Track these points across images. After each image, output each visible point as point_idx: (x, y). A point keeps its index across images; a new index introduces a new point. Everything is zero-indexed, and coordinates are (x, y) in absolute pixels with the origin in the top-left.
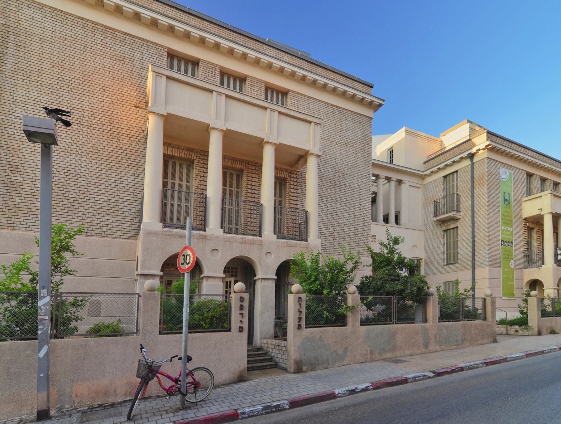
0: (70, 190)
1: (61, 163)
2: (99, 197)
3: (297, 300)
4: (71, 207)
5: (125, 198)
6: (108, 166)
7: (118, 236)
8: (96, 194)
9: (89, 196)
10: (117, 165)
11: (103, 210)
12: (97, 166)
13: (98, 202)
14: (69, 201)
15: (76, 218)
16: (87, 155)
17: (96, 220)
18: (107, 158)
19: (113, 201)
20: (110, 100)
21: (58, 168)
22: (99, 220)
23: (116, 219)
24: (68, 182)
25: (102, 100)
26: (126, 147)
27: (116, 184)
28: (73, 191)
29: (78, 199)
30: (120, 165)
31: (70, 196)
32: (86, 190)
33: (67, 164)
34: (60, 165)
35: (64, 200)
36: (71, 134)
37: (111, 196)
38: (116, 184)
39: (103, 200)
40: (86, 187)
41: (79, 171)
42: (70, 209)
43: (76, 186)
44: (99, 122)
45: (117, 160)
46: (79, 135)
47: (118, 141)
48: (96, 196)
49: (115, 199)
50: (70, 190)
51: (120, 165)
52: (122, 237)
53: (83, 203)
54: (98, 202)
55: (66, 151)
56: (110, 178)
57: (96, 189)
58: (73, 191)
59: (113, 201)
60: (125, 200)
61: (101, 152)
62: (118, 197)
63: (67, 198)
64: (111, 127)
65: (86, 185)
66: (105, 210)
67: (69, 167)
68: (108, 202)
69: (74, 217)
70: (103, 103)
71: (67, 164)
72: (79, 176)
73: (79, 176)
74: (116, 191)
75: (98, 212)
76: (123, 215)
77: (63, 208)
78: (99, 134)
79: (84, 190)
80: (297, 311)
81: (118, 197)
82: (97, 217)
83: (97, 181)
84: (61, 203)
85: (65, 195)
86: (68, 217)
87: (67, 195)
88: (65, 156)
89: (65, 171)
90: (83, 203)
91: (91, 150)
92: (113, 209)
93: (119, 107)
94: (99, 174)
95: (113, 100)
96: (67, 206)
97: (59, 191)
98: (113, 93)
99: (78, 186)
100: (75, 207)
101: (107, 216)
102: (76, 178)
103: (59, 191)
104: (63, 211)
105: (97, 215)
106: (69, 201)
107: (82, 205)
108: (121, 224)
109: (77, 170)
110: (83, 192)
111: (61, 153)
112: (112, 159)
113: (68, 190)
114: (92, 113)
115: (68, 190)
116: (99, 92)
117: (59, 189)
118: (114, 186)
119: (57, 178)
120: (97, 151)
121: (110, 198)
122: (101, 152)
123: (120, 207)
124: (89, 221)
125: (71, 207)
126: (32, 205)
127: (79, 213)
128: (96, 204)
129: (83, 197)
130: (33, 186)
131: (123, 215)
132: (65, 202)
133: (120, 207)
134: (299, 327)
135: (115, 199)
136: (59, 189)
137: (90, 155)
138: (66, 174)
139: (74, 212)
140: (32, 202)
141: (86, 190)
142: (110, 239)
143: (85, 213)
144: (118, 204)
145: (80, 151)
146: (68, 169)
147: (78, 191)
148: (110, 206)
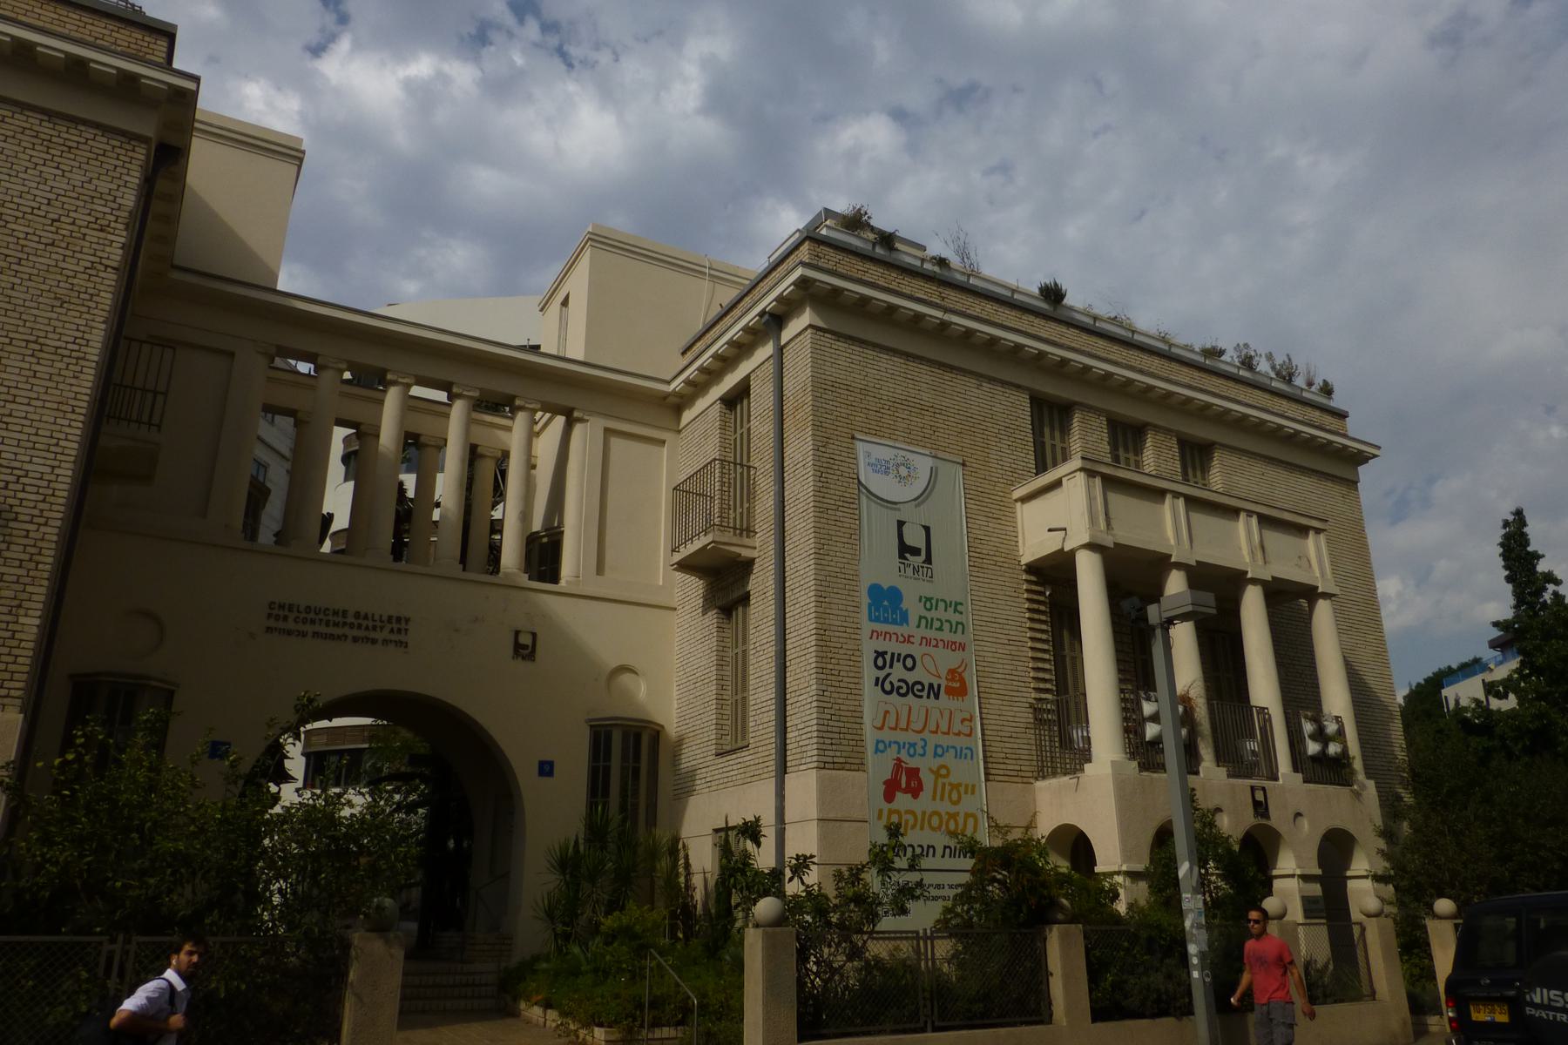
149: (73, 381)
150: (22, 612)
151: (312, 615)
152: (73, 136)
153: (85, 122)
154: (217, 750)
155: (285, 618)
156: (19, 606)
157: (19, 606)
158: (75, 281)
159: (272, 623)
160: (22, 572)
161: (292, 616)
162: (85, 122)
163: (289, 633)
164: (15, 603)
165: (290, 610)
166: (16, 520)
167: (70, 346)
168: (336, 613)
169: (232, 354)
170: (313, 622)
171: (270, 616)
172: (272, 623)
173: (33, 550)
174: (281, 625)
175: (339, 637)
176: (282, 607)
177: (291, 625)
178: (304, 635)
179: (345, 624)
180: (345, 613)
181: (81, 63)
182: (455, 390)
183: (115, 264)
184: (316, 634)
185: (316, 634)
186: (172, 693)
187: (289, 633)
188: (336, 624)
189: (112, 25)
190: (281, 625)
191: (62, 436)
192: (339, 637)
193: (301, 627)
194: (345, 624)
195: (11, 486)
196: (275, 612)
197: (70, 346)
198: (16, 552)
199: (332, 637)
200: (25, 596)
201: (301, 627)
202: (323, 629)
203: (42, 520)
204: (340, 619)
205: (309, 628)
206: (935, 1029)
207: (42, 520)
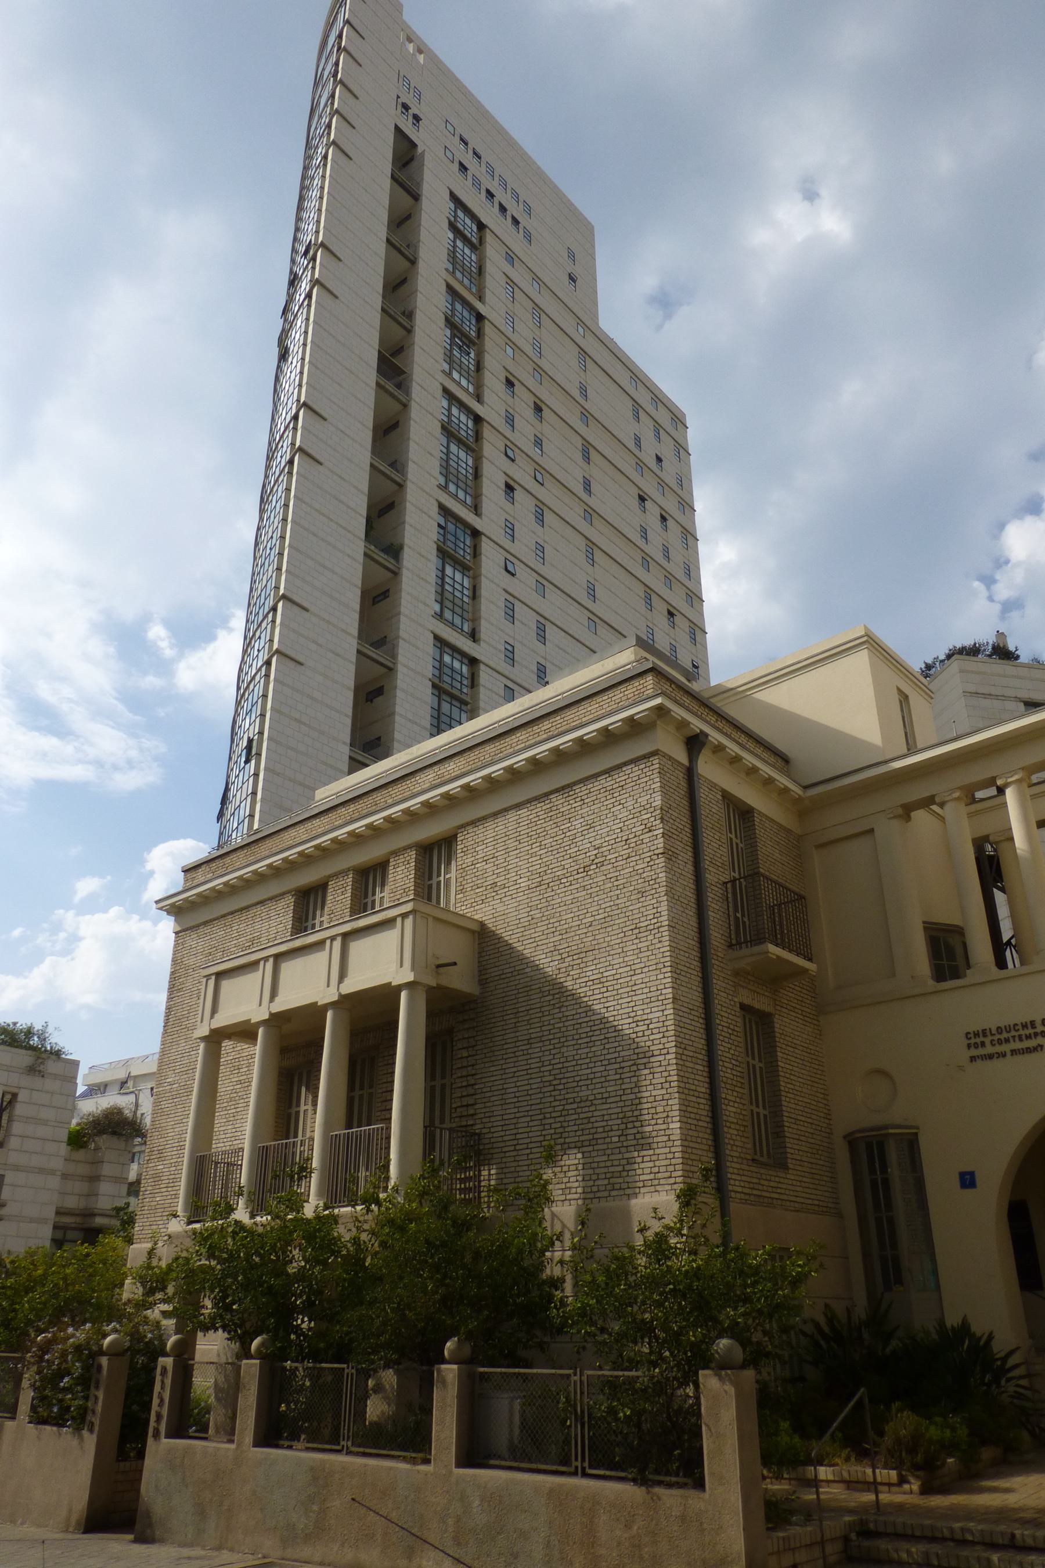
149: (659, 945)
150: (670, 1120)
151: (1005, 1035)
152: (620, 777)
153: (625, 764)
154: (968, 1180)
155: (983, 1044)
156: (668, 1116)
157: (668, 1116)
158: (645, 875)
159: (974, 1052)
160: (664, 1091)
161: (987, 1040)
162: (625, 764)
163: (990, 1057)
164: (665, 1115)
165: (985, 1035)
166: (653, 1056)
167: (653, 921)
168: (1024, 1026)
169: (871, 831)
170: (1007, 1040)
171: (969, 1046)
172: (974, 1052)
173: (665, 1074)
174: (981, 1051)
175: (1035, 1049)
176: (976, 1035)
177: (989, 1049)
178: (1004, 1055)
179: (1036, 1034)
180: (1033, 1024)
181: (605, 730)
182: (999, 782)
183: (661, 851)
184: (1014, 1052)
185: (1014, 1052)
186: (916, 1134)
187: (990, 1057)
188: (1028, 1037)
189: (622, 688)
190: (981, 1051)
191: (662, 987)
192: (1035, 1049)
193: (999, 1049)
194: (1036, 1034)
195: (646, 1033)
196: (973, 1041)
197: (653, 921)
198: (659, 1079)
199: (1029, 1050)
200: (668, 1108)
201: (999, 1049)
202: (1018, 1045)
203: (665, 1051)
204: (1031, 1031)
205: (1006, 1048)
206: (584, 1475)
207: (665, 1051)
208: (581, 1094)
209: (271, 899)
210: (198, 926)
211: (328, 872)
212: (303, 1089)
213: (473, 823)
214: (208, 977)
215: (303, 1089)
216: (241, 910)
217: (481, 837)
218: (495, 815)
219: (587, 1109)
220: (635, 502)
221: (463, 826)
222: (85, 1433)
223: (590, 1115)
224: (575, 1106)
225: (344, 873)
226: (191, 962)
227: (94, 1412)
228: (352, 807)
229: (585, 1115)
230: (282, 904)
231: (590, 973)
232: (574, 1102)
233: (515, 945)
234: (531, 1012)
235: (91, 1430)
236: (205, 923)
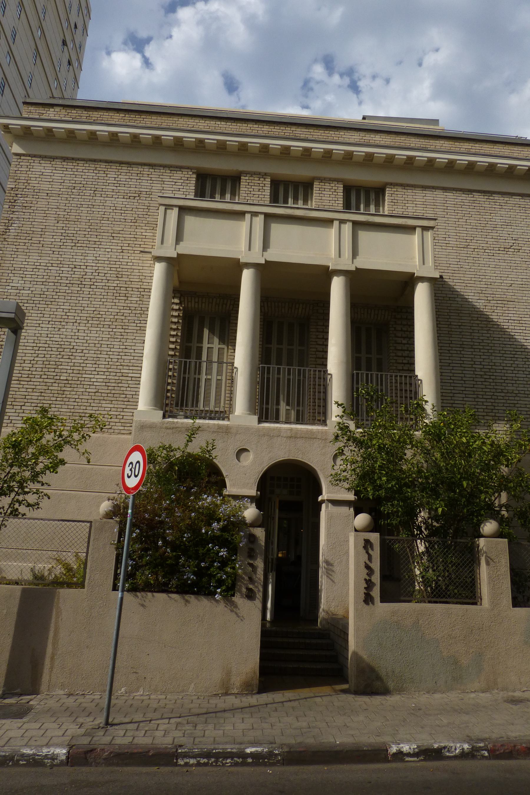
0: (62, 371)
1: (55, 336)
2: (96, 376)
3: (362, 543)
4: (61, 392)
5: (130, 375)
6: (111, 333)
7: (116, 431)
8: (93, 373)
9: (84, 376)
10: (123, 330)
11: (100, 394)
12: (97, 335)
13: (95, 384)
14: (60, 385)
15: (66, 407)
16: (86, 322)
17: (91, 408)
18: (110, 323)
19: (114, 381)
20: (120, 248)
21: (51, 342)
22: (94, 408)
23: (116, 406)
24: (61, 360)
25: (110, 250)
26: (135, 305)
27: (119, 357)
28: (65, 371)
29: (70, 382)
30: (126, 331)
31: (62, 378)
32: (81, 368)
33: (62, 336)
34: (53, 339)
35: (54, 384)
36: (69, 298)
37: (112, 374)
38: (119, 357)
39: (102, 380)
40: (82, 365)
41: (75, 344)
42: (60, 396)
43: (70, 364)
44: (104, 278)
45: (122, 324)
46: (78, 298)
47: (125, 298)
48: (92, 376)
49: (116, 378)
50: (62, 371)
51: (126, 331)
52: (123, 432)
53: (76, 386)
54: (95, 384)
55: (62, 320)
56: (112, 350)
57: (94, 366)
58: (65, 371)
59: (114, 381)
60: (130, 379)
61: (104, 316)
62: (120, 374)
63: (57, 381)
64: (118, 282)
65: (82, 361)
66: (103, 395)
67: (64, 340)
68: (106, 383)
69: (63, 406)
70: (110, 253)
71: (62, 336)
72: (74, 351)
73: (74, 351)
74: (119, 367)
75: (93, 398)
76: (126, 400)
77: (51, 395)
78: (103, 294)
79: (79, 368)
80: (363, 566)
81: (120, 374)
82: (92, 405)
83: (95, 355)
84: (50, 388)
85: (55, 378)
86: (57, 406)
87: (58, 377)
88: (60, 327)
89: (58, 346)
90: (76, 386)
91: (92, 315)
92: (113, 392)
93: (129, 255)
94: (99, 345)
95: (123, 248)
96: (56, 392)
97: (49, 373)
98: (123, 239)
99: (72, 364)
100: (66, 393)
101: (104, 402)
102: (70, 354)
103: (49, 373)
104: (52, 399)
105: (92, 401)
106: (60, 385)
107: (75, 389)
108: (122, 414)
109: (72, 344)
110: (78, 372)
111: (56, 323)
112: (116, 323)
113: (59, 371)
114: (97, 268)
115: (59, 371)
116: (107, 240)
117: (50, 370)
118: (116, 360)
119: (49, 356)
120: (98, 316)
121: (110, 377)
122: (104, 316)
123: (122, 389)
124: (82, 411)
125: (61, 392)
126: (17, 393)
127: (71, 400)
128: (91, 387)
129: (76, 379)
130: (21, 368)
131: (126, 400)
132: (55, 387)
133: (122, 389)
134: (368, 599)
135: (116, 378)
136: (50, 370)
137: (90, 322)
138: (59, 350)
139: (65, 399)
140: (17, 390)
141: (81, 368)
142: (106, 435)
143: (77, 400)
144: (120, 385)
145: (79, 318)
146: (62, 343)
147: (71, 371)
148: (110, 388)
208: (507, 388)
209: (164, 166)
210: (54, 158)
211: (241, 168)
212: (206, 332)
213: (404, 186)
214: (168, 207)
215: (206, 332)
216: (121, 163)
217: (410, 198)
218: (424, 188)
219: (513, 398)
220: (61, 43)
221: (391, 184)
222: (237, 599)
223: (516, 402)
224: (503, 394)
225: (264, 175)
226: (45, 186)
227: (251, 580)
228: (266, 129)
229: (512, 402)
230: (178, 175)
231: (512, 315)
232: (502, 392)
233: (447, 280)
234: (462, 327)
235: (250, 595)
236: (65, 159)
